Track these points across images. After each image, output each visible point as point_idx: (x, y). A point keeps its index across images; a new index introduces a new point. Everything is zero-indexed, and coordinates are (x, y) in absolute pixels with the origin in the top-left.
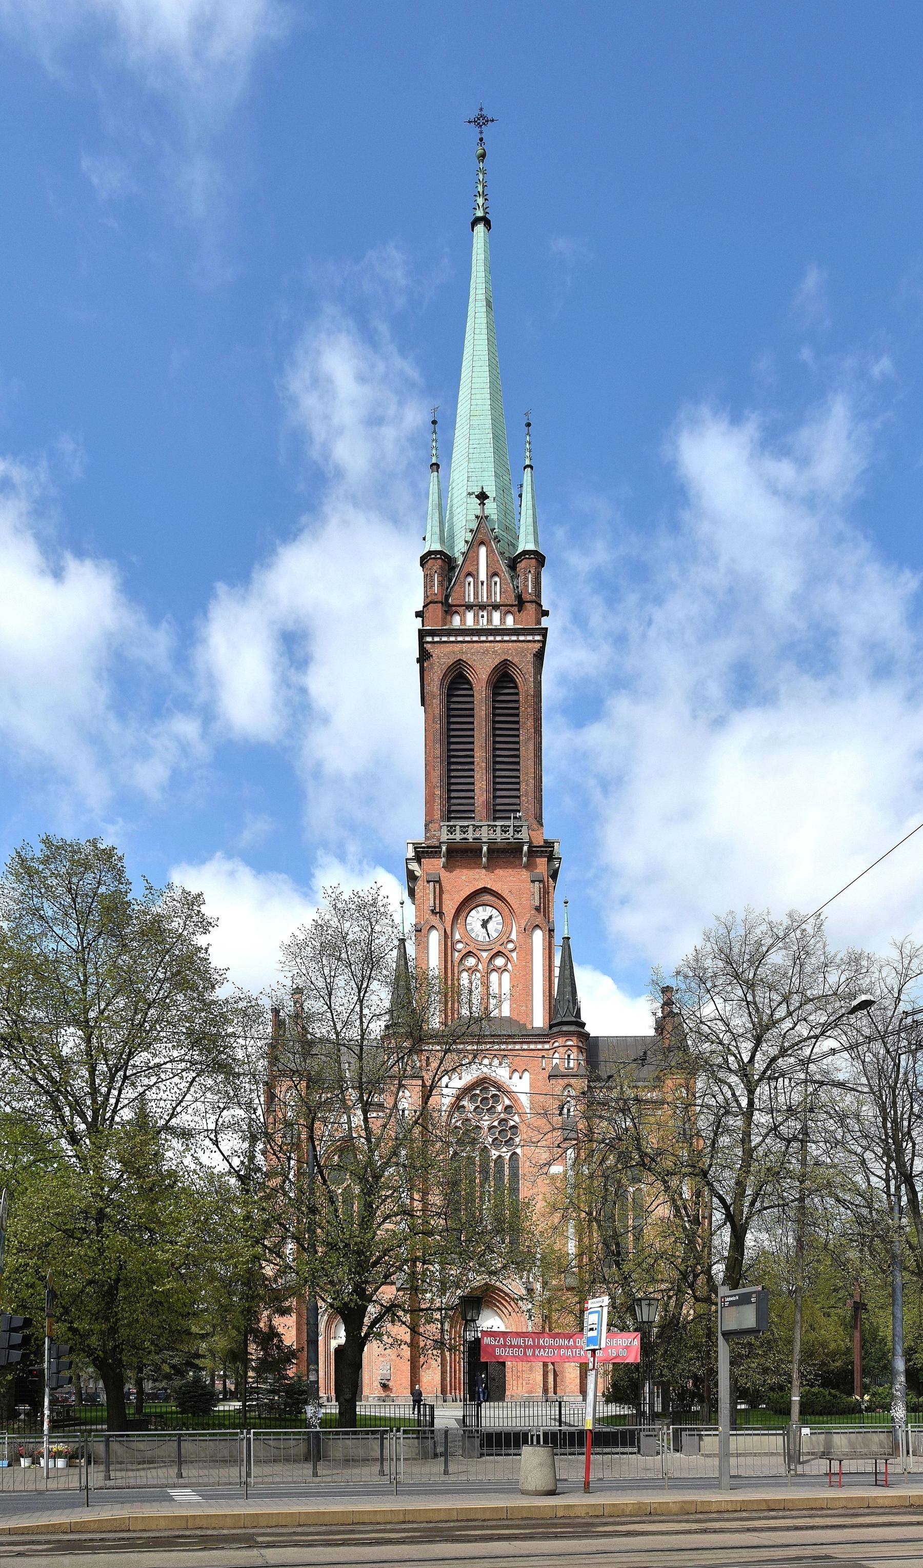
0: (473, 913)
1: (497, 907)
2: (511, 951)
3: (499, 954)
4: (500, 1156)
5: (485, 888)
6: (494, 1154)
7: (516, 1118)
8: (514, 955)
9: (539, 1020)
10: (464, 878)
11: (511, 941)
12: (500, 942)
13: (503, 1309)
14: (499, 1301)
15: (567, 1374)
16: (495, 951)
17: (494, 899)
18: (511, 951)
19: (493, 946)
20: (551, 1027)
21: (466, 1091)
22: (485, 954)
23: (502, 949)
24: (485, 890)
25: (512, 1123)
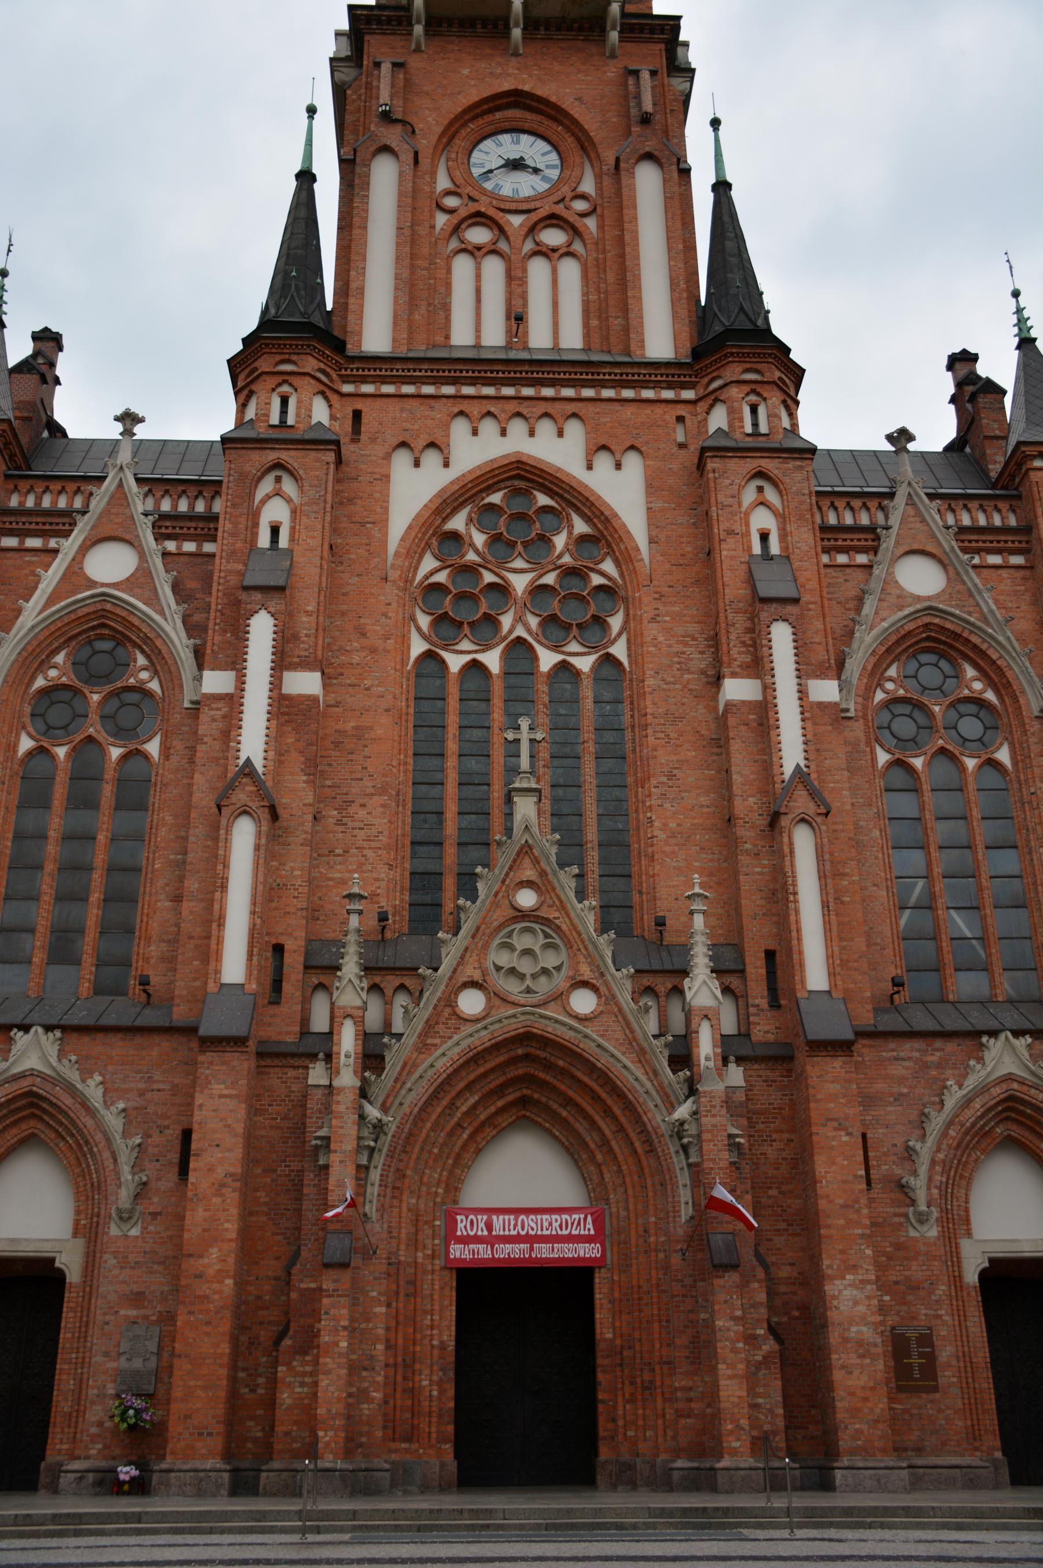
0: (488, 144)
1: (548, 133)
2: (583, 215)
3: (554, 220)
4: (563, 666)
5: (516, 93)
6: (547, 659)
7: (608, 566)
8: (591, 223)
9: (660, 339)
10: (466, 72)
11: (583, 197)
12: (557, 197)
13: (581, 1126)
14: (568, 1102)
15: (837, 1375)
16: (542, 213)
17: (539, 118)
18: (583, 215)
19: (538, 204)
20: (697, 354)
21: (468, 493)
22: (516, 220)
23: (559, 209)
24: (517, 99)
25: (597, 580)
